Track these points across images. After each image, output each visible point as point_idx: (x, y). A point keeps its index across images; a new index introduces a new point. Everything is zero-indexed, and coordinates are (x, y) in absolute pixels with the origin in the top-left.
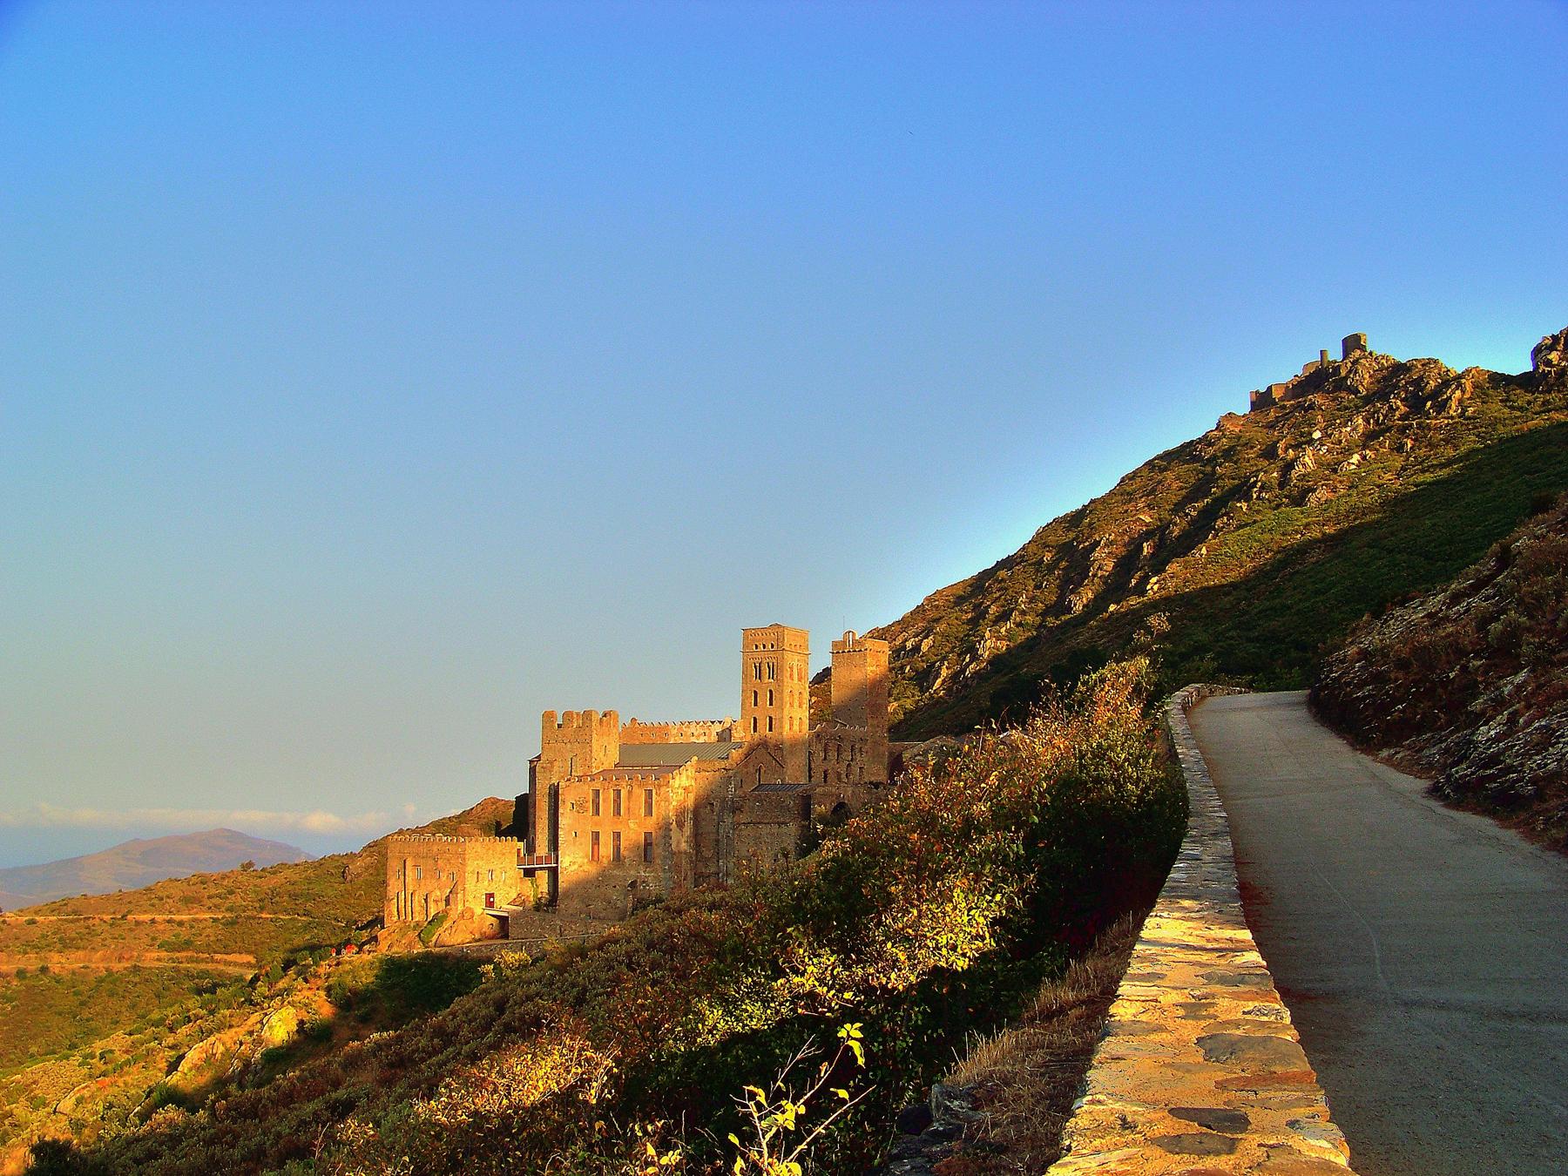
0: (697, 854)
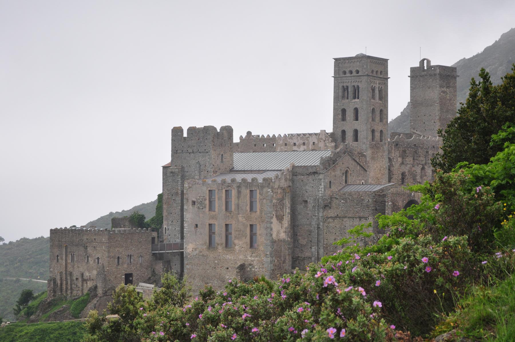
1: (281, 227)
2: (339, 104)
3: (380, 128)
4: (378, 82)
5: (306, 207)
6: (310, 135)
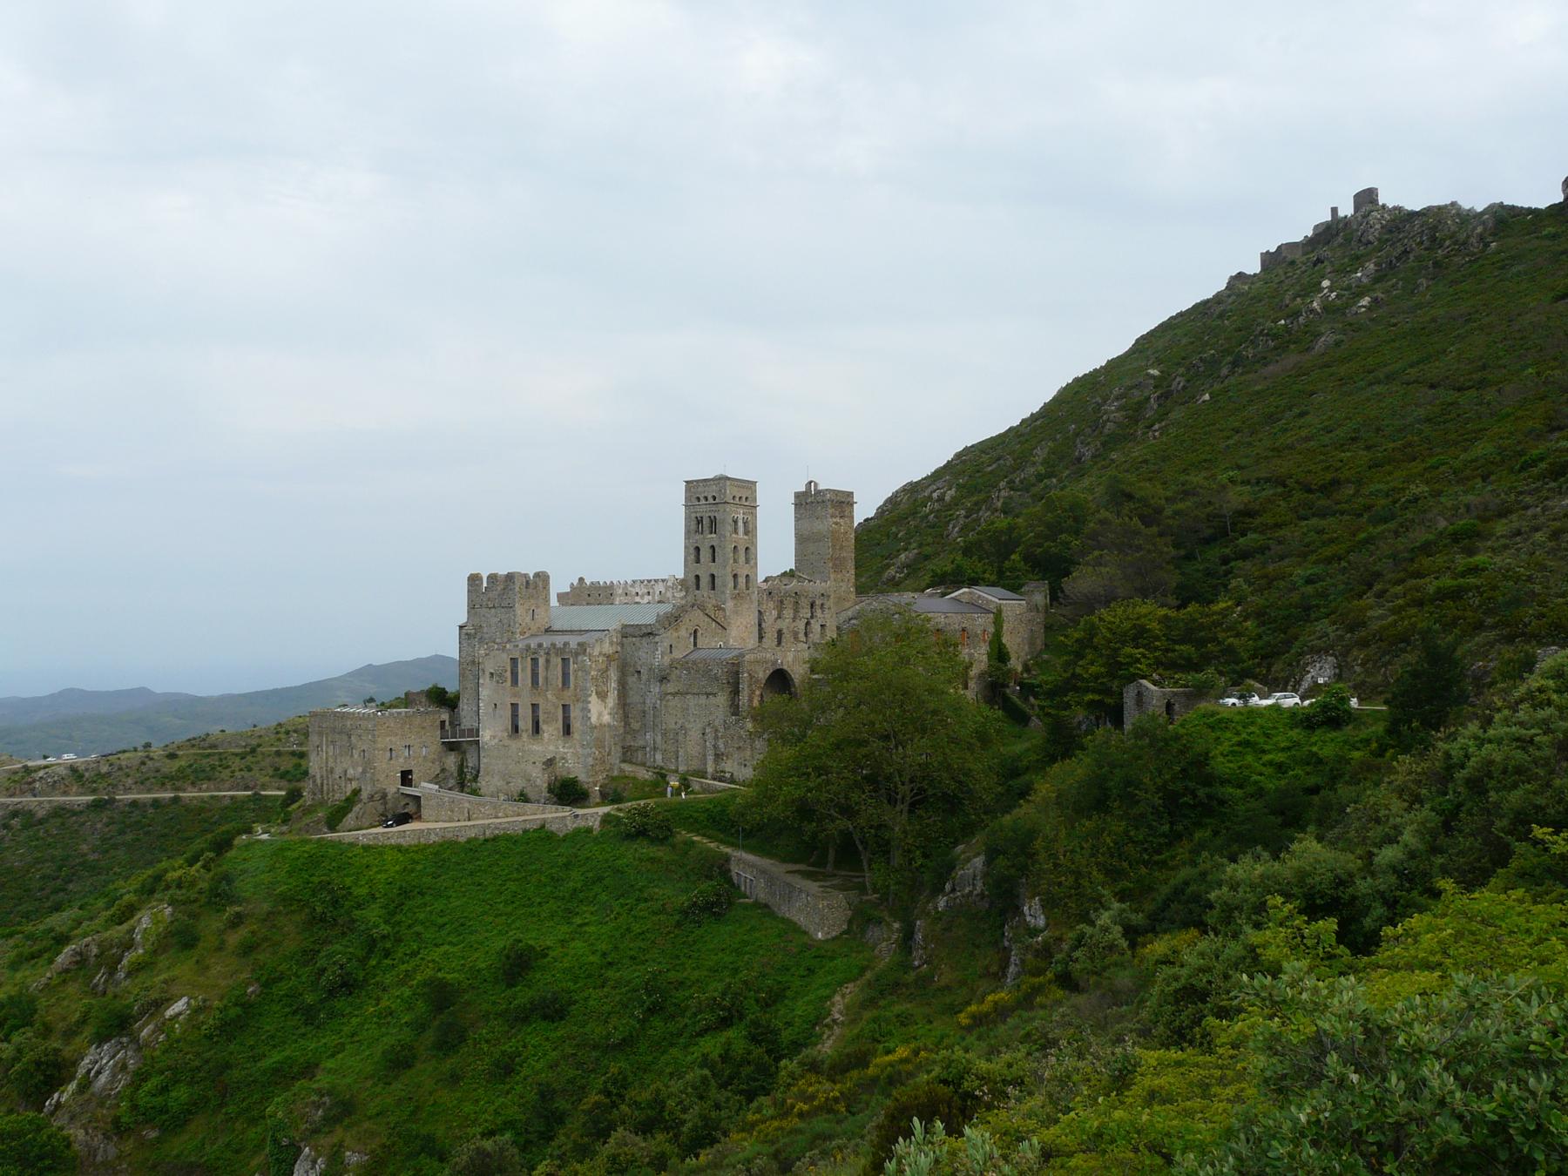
0: (625, 727)
5: (640, 679)
6: (656, 581)
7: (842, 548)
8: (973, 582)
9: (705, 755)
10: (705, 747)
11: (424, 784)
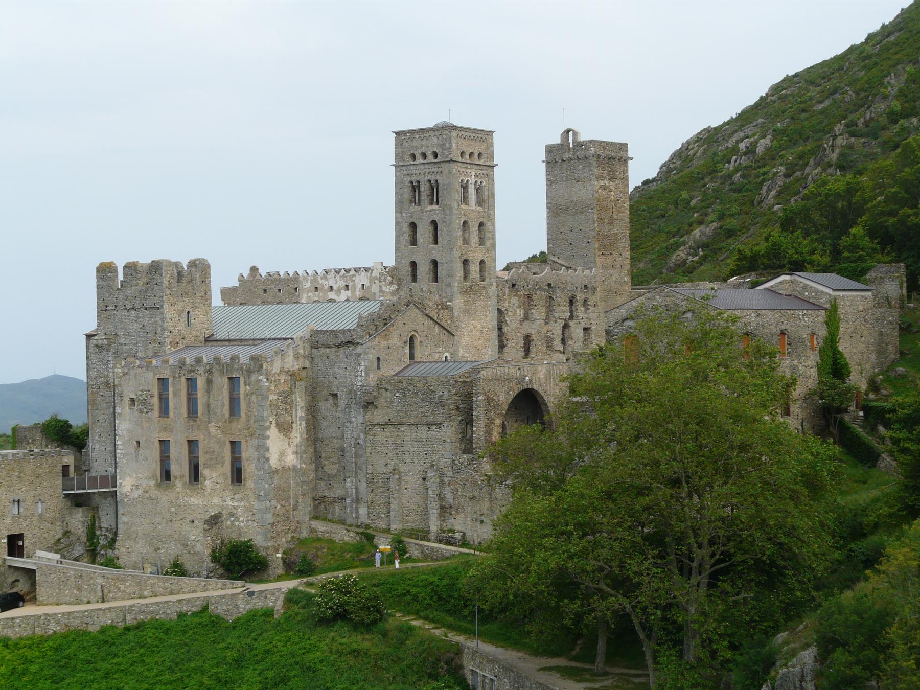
0: (317, 470)
1: (289, 444)
2: (404, 214)
3: (480, 257)
4: (473, 174)
6: (357, 270)
7: (612, 222)
8: (797, 267)
9: (426, 509)
10: (426, 498)
11: (40, 553)
